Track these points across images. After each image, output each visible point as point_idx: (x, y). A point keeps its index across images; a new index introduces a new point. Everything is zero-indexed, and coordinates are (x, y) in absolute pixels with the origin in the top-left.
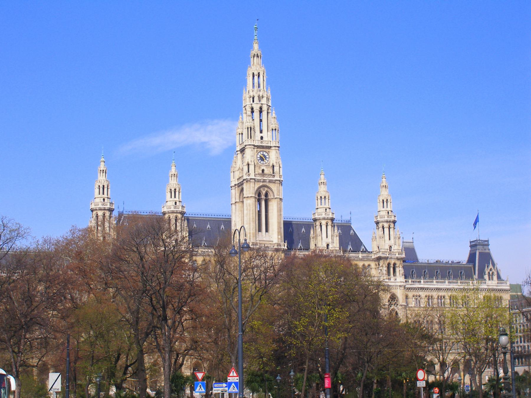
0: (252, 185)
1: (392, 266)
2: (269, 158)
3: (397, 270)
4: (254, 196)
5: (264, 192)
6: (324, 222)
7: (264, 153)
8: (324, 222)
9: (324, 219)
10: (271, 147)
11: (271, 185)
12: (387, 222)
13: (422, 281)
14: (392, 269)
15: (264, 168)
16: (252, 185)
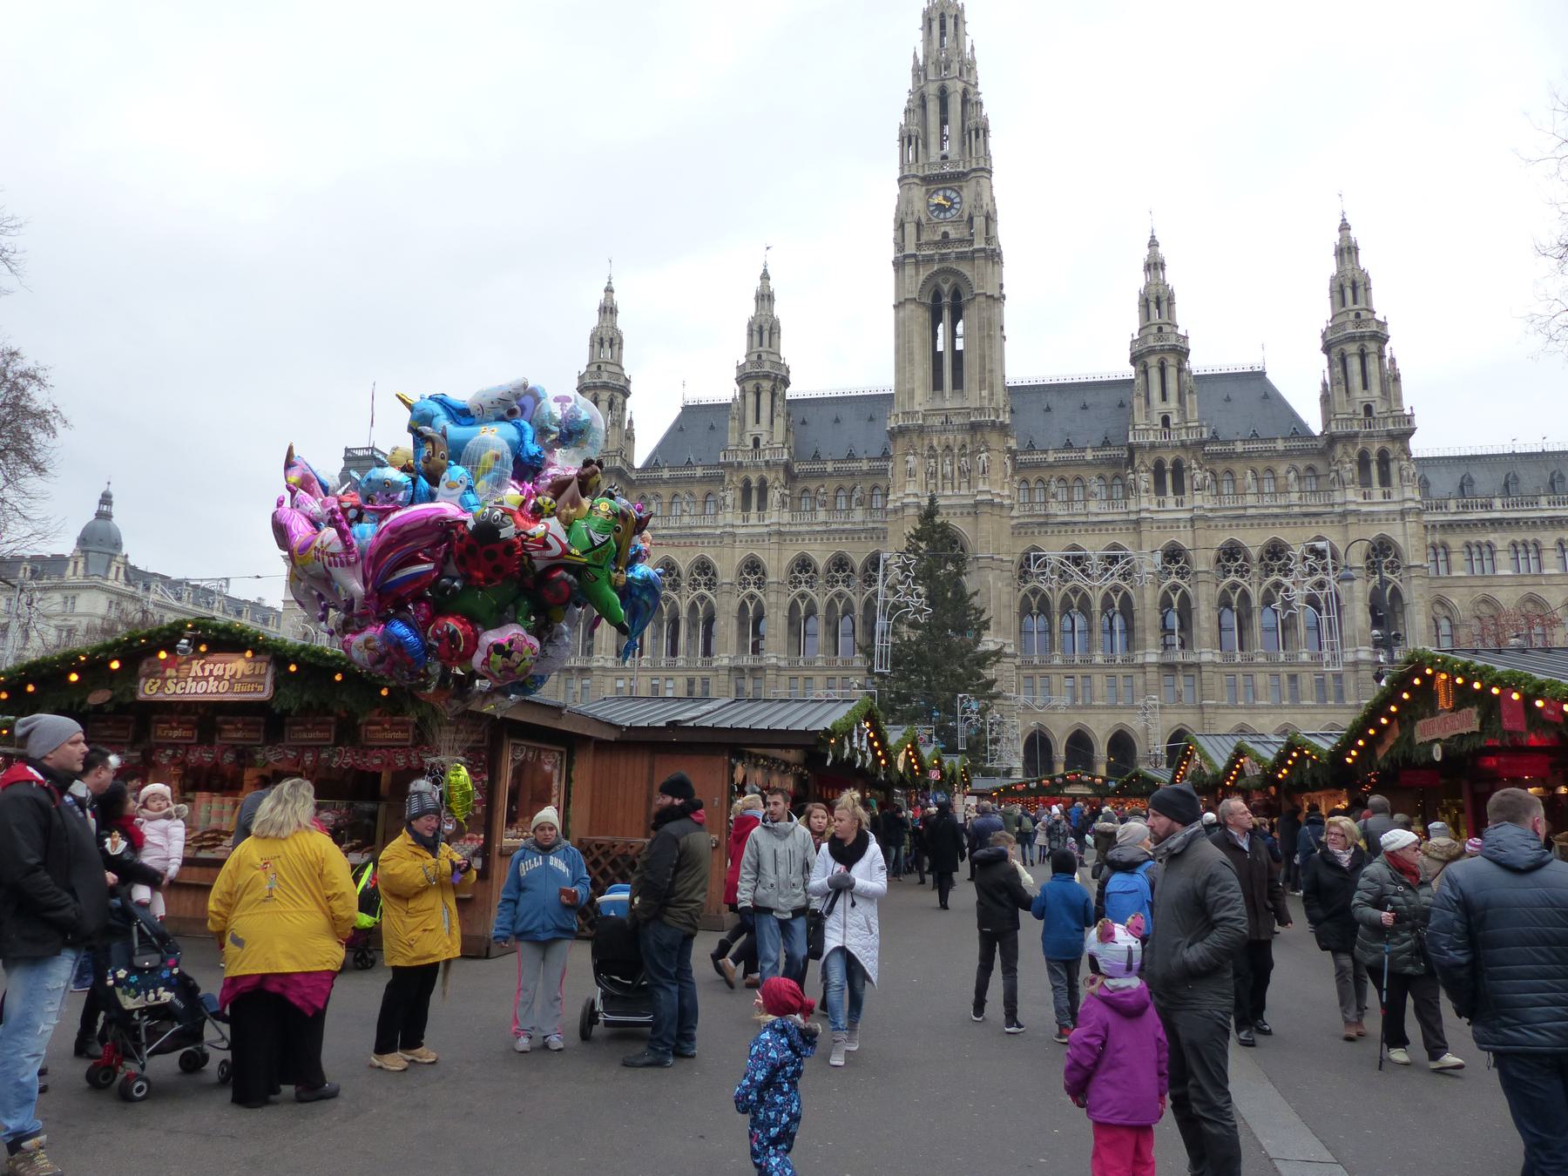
0: (910, 270)
1: (1374, 457)
2: (961, 203)
3: (1394, 467)
4: (915, 295)
5: (946, 288)
6: (1153, 361)
7: (948, 193)
8: (1153, 361)
9: (1152, 351)
10: (964, 175)
11: (964, 268)
12: (1352, 338)
13: (1498, 503)
14: (1374, 469)
15: (947, 229)
16: (910, 270)
